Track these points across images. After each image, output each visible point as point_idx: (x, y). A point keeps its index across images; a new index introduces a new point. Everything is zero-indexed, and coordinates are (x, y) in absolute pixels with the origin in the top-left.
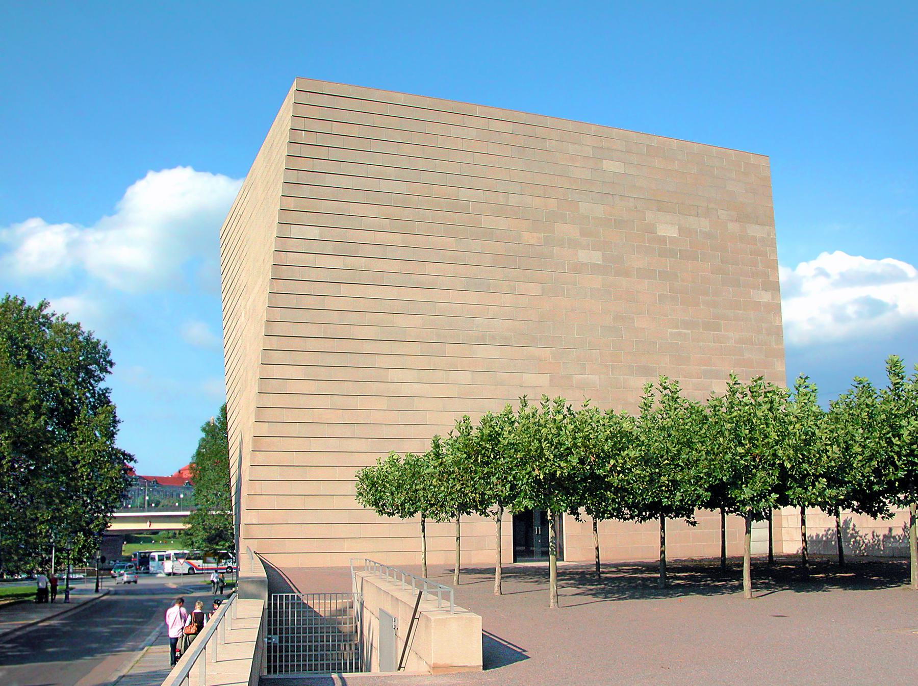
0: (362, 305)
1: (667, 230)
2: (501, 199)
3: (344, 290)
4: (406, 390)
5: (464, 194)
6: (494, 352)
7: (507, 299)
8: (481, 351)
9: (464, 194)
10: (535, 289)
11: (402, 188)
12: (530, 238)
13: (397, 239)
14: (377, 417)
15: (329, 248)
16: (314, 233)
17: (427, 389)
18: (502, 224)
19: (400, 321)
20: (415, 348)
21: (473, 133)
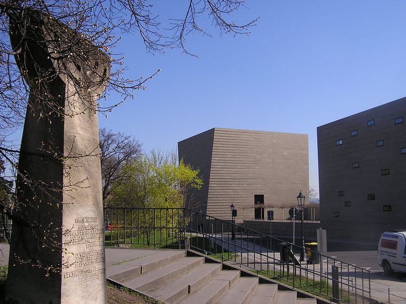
0: (227, 172)
1: (285, 154)
2: (253, 149)
3: (225, 169)
4: (235, 188)
5: (246, 149)
6: (251, 180)
7: (254, 170)
8: (249, 180)
9: (246, 149)
10: (259, 168)
11: (234, 149)
12: (258, 157)
13: (233, 159)
14: (231, 193)
15: (221, 161)
16: (218, 159)
17: (238, 188)
18: (252, 155)
19: (234, 175)
20: (237, 180)
21: (247, 136)
